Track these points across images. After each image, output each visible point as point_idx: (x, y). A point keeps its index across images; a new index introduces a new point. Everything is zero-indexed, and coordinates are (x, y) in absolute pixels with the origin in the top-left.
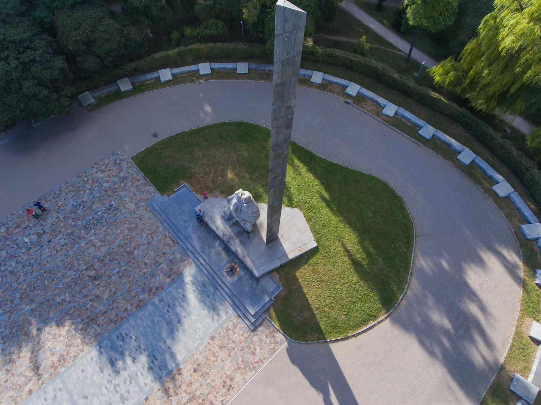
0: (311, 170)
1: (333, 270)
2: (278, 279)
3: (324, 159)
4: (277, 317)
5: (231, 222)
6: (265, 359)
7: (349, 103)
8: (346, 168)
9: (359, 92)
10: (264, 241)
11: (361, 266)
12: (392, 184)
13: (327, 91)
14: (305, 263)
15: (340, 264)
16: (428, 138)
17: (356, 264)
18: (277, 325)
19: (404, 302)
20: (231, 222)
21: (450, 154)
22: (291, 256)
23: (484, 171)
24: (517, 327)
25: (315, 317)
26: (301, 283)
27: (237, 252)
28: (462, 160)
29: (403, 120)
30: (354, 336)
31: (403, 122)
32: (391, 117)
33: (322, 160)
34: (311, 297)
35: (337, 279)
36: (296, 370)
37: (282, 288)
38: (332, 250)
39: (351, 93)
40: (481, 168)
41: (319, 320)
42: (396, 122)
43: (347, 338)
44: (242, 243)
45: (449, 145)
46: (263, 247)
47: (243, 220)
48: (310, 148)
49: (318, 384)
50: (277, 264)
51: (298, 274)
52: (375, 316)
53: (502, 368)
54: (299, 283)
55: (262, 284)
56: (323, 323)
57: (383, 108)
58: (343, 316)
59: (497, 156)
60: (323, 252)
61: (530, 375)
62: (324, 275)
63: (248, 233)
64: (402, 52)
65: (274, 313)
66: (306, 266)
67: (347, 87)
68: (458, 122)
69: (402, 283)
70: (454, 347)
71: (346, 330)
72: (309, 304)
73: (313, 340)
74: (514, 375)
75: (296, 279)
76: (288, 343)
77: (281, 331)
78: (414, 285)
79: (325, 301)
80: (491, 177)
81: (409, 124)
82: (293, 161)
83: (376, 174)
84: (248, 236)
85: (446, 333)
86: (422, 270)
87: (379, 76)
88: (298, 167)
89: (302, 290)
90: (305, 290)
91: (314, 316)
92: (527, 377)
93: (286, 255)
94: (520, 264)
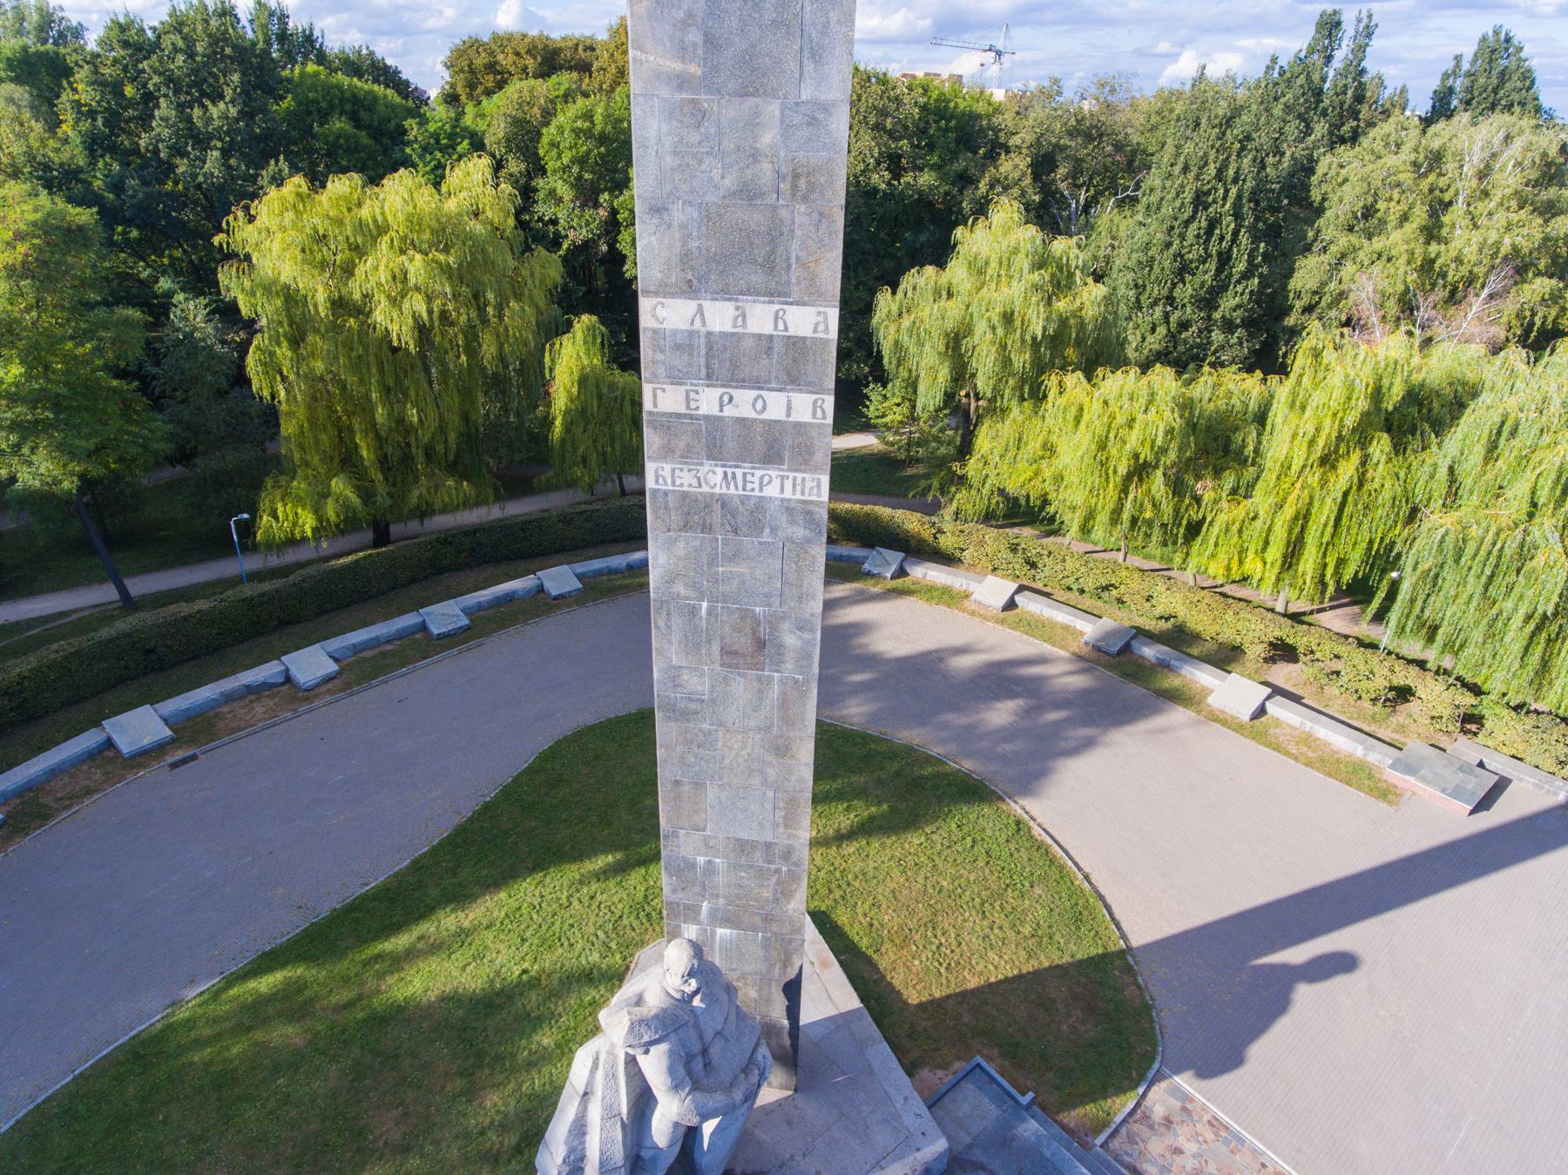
0: (459, 897)
1: (893, 885)
2: (940, 1073)
3: (414, 863)
4: (1094, 1101)
6: (1264, 1165)
7: (193, 758)
8: (486, 807)
9: (165, 720)
11: (872, 818)
12: (588, 718)
13: (66, 808)
15: (871, 864)
16: (465, 621)
17: (865, 830)
18: (1123, 1104)
19: (967, 765)
21: (540, 604)
22: (849, 1000)
23: (610, 571)
24: (985, 618)
25: (1058, 966)
28: (567, 589)
29: (366, 654)
30: (1087, 877)
31: (374, 657)
32: (340, 673)
33: (417, 866)
35: (921, 879)
36: (1258, 1050)
37: (979, 1059)
38: (822, 874)
39: (147, 741)
40: (598, 573)
41: (1066, 959)
42: (359, 671)
43: (1101, 898)
45: (510, 598)
46: (810, 1108)
47: (745, 1070)
48: (328, 904)
49: (1270, 998)
50: (881, 1054)
51: (913, 997)
52: (1018, 823)
53: (1079, 657)
54: (948, 997)
55: (969, 1146)
56: (1073, 947)
57: (288, 679)
58: (1038, 891)
59: (576, 548)
60: (829, 902)
62: (912, 913)
64: (75, 611)
65: (1080, 1111)
66: (883, 964)
67: (109, 743)
68: (441, 571)
69: (910, 754)
70: (1056, 705)
71: (1074, 892)
72: (1020, 977)
73: (1139, 987)
74: (1086, 643)
75: (933, 1007)
76: (1178, 1070)
77: (1141, 1090)
78: (911, 735)
79: (1001, 928)
80: (630, 567)
81: (389, 647)
82: (379, 957)
83: (543, 742)
85: (1028, 712)
86: (875, 717)
87: (149, 652)
88: (421, 938)
90: (973, 982)
91: (1058, 972)
92: (1082, 634)
93: (847, 1017)
94: (848, 586)
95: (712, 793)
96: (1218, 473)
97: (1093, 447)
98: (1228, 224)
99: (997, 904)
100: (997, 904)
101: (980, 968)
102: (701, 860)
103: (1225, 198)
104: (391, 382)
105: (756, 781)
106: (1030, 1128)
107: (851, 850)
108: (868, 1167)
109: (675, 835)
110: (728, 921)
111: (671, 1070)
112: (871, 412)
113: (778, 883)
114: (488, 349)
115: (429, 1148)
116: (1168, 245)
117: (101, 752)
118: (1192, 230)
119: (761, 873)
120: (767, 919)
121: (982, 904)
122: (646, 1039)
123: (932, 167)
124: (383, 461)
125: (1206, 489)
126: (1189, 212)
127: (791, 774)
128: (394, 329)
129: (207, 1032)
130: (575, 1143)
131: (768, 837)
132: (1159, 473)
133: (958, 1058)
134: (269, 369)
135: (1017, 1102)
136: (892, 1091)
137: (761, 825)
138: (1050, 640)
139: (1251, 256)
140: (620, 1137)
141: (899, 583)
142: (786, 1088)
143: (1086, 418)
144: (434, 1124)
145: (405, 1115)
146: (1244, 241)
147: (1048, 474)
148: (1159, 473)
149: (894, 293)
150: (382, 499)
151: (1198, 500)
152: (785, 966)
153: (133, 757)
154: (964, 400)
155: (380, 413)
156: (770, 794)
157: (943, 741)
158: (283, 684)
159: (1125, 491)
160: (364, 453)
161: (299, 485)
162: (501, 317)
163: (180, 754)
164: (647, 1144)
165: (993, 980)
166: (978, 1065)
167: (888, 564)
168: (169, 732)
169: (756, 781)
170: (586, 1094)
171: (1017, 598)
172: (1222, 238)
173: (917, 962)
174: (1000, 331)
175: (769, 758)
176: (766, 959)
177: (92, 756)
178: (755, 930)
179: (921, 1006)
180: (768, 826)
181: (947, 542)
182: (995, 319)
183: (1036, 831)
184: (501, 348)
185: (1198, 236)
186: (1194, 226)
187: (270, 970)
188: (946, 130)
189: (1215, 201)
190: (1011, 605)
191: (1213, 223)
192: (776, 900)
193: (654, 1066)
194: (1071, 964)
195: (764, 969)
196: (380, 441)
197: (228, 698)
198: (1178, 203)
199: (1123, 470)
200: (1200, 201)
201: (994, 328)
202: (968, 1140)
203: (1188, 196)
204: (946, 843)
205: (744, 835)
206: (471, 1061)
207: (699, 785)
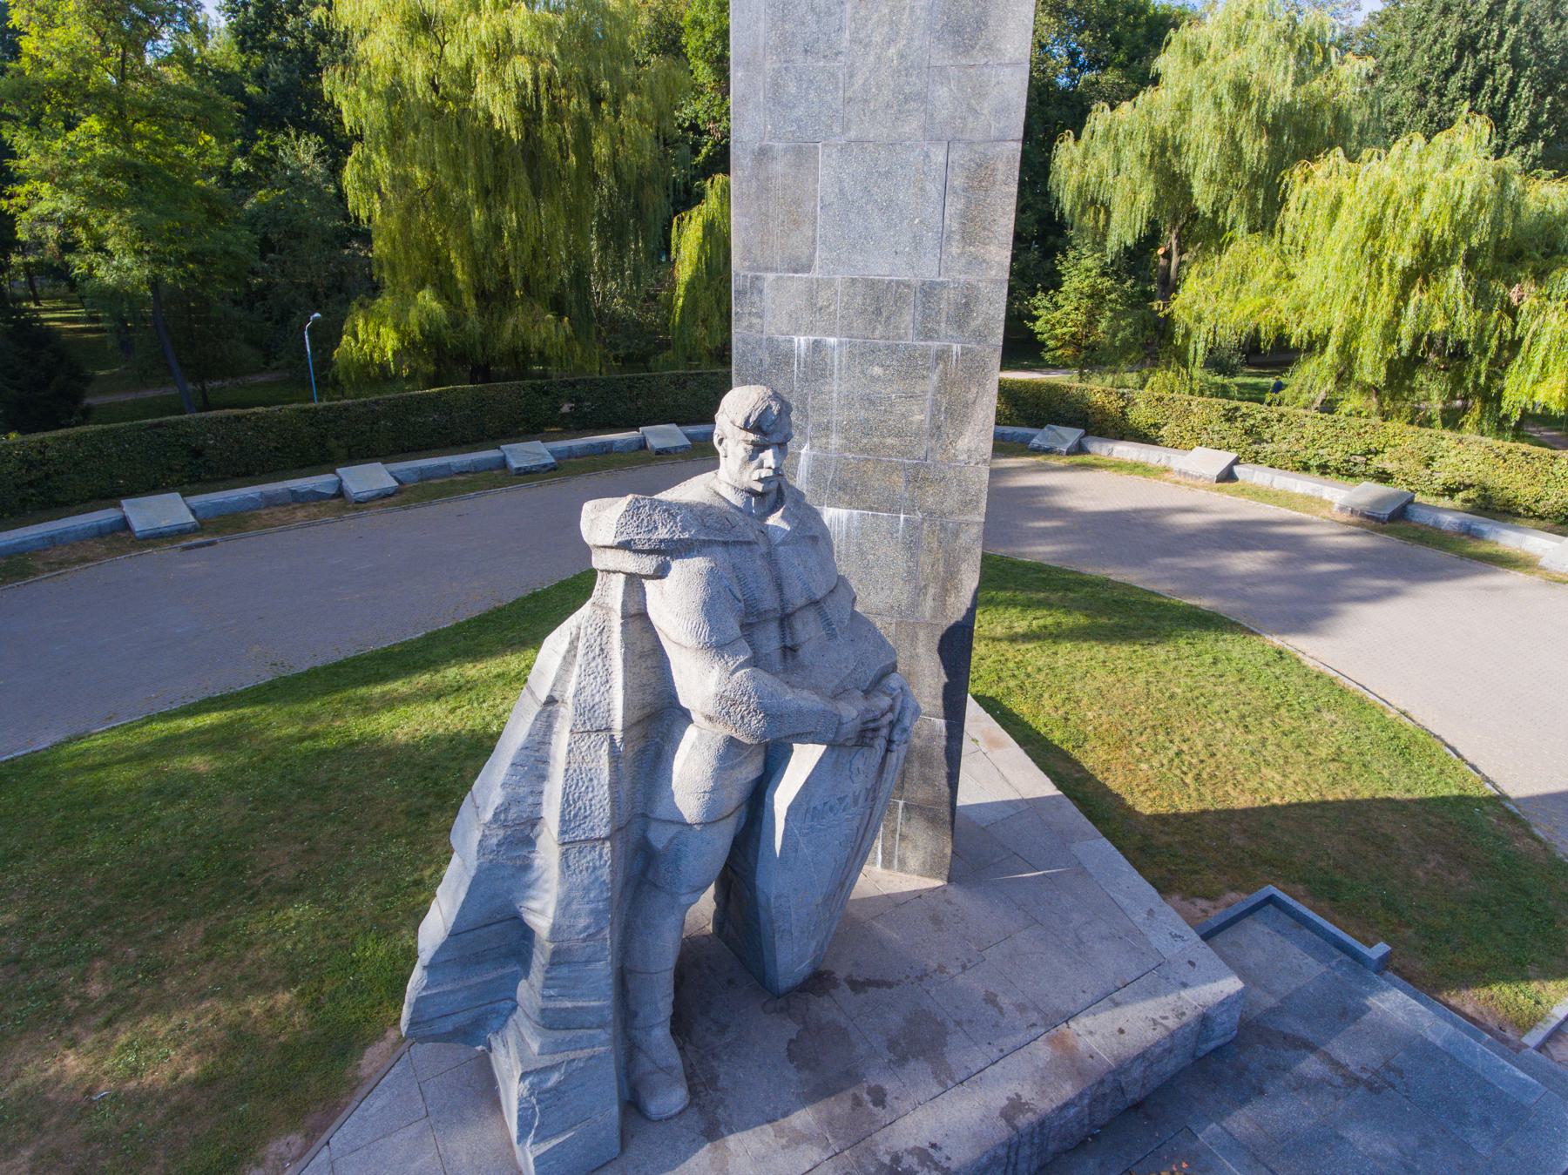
2: (1203, 904)
5: (670, 1098)
10: (918, 895)
14: (1066, 757)
20: (670, 1098)
22: (1036, 784)
26: (1197, 807)
27: (1016, 1105)
32: (397, 492)
34: (1280, 788)
38: (988, 662)
44: (924, 1043)
45: (606, 449)
51: (1145, 806)
55: (1271, 1010)
57: (340, 493)
61: (1326, 497)
63: (818, 981)
66: (1088, 763)
67: (124, 524)
84: (856, 986)
87: (197, 453)
89: (1245, 812)
90: (1242, 801)
93: (1034, 806)
95: (828, 171)
96: (1540, 276)
97: (1362, 233)
98: (1505, 72)
99: (1267, 722)
100: (1267, 722)
101: (1253, 784)
102: (801, 342)
103: (1499, 45)
104: (489, 181)
105: (911, 126)
106: (1393, 1004)
107: (1030, 646)
108: (1089, 998)
109: (755, 285)
110: (847, 490)
111: (711, 609)
112: (1039, 326)
113: (945, 385)
114: (601, 148)
115: (328, 893)
116: (1421, 106)
117: (112, 532)
118: (1455, 82)
119: (909, 365)
120: (918, 477)
121: (1243, 717)
122: (663, 533)
123: (1116, 66)
124: (481, 295)
125: (1525, 294)
126: (1451, 58)
127: (982, 96)
128: (496, 111)
129: (98, 759)
130: (523, 791)
131: (929, 271)
132: (1456, 271)
133: (1233, 889)
134: (369, 187)
135: (1356, 956)
136: (1125, 901)
137: (917, 241)
138: (1288, 506)
139: (1534, 116)
140: (605, 776)
141: (1078, 459)
142: (930, 870)
143: (1343, 213)
144: (349, 864)
145: (312, 850)
146: (1525, 94)
147: (1283, 302)
148: (1456, 271)
149: (1077, 138)
150: (473, 323)
151: (1512, 312)
152: (944, 592)
153: (146, 538)
154: (1162, 262)
155: (477, 215)
156: (939, 156)
157: (1155, 581)
158: (334, 497)
159: (1404, 296)
160: (459, 276)
161: (385, 302)
162: (617, 113)
163: (200, 540)
164: (661, 811)
165: (1276, 801)
166: (1271, 899)
167: (1066, 441)
168: (192, 519)
169: (911, 126)
170: (551, 701)
171: (1236, 469)
172: (1495, 91)
173: (1144, 766)
174: (1228, 107)
175: (941, 57)
176: (911, 575)
177: (101, 533)
178: (892, 506)
179: (1158, 818)
180: (930, 239)
181: (1140, 414)
182: (1223, 89)
183: (1307, 661)
184: (615, 153)
185: (1463, 88)
186: (1460, 74)
187: (208, 711)
188: (1135, 26)
189: (1486, 47)
190: (1228, 476)
191: (1485, 72)
192: (936, 431)
193: (675, 603)
194: (1411, 801)
195: (905, 599)
196: (476, 265)
197: (270, 501)
198: (1436, 49)
199: (1405, 258)
200: (1467, 45)
201: (1218, 104)
202: (1271, 1001)
203: (1450, 41)
204: (1172, 656)
205: (882, 268)
206: (430, 800)
207: (802, 154)
